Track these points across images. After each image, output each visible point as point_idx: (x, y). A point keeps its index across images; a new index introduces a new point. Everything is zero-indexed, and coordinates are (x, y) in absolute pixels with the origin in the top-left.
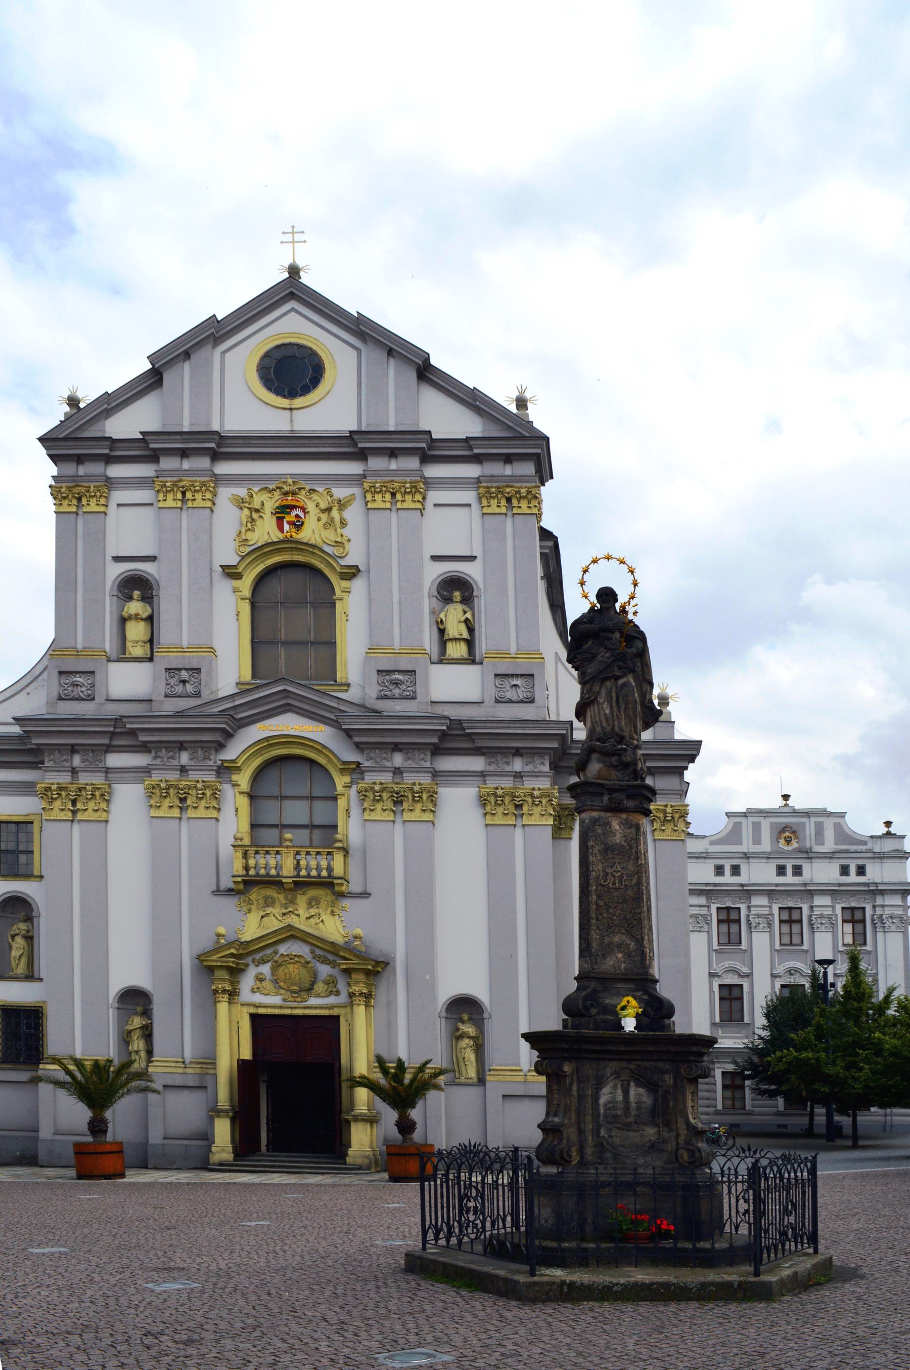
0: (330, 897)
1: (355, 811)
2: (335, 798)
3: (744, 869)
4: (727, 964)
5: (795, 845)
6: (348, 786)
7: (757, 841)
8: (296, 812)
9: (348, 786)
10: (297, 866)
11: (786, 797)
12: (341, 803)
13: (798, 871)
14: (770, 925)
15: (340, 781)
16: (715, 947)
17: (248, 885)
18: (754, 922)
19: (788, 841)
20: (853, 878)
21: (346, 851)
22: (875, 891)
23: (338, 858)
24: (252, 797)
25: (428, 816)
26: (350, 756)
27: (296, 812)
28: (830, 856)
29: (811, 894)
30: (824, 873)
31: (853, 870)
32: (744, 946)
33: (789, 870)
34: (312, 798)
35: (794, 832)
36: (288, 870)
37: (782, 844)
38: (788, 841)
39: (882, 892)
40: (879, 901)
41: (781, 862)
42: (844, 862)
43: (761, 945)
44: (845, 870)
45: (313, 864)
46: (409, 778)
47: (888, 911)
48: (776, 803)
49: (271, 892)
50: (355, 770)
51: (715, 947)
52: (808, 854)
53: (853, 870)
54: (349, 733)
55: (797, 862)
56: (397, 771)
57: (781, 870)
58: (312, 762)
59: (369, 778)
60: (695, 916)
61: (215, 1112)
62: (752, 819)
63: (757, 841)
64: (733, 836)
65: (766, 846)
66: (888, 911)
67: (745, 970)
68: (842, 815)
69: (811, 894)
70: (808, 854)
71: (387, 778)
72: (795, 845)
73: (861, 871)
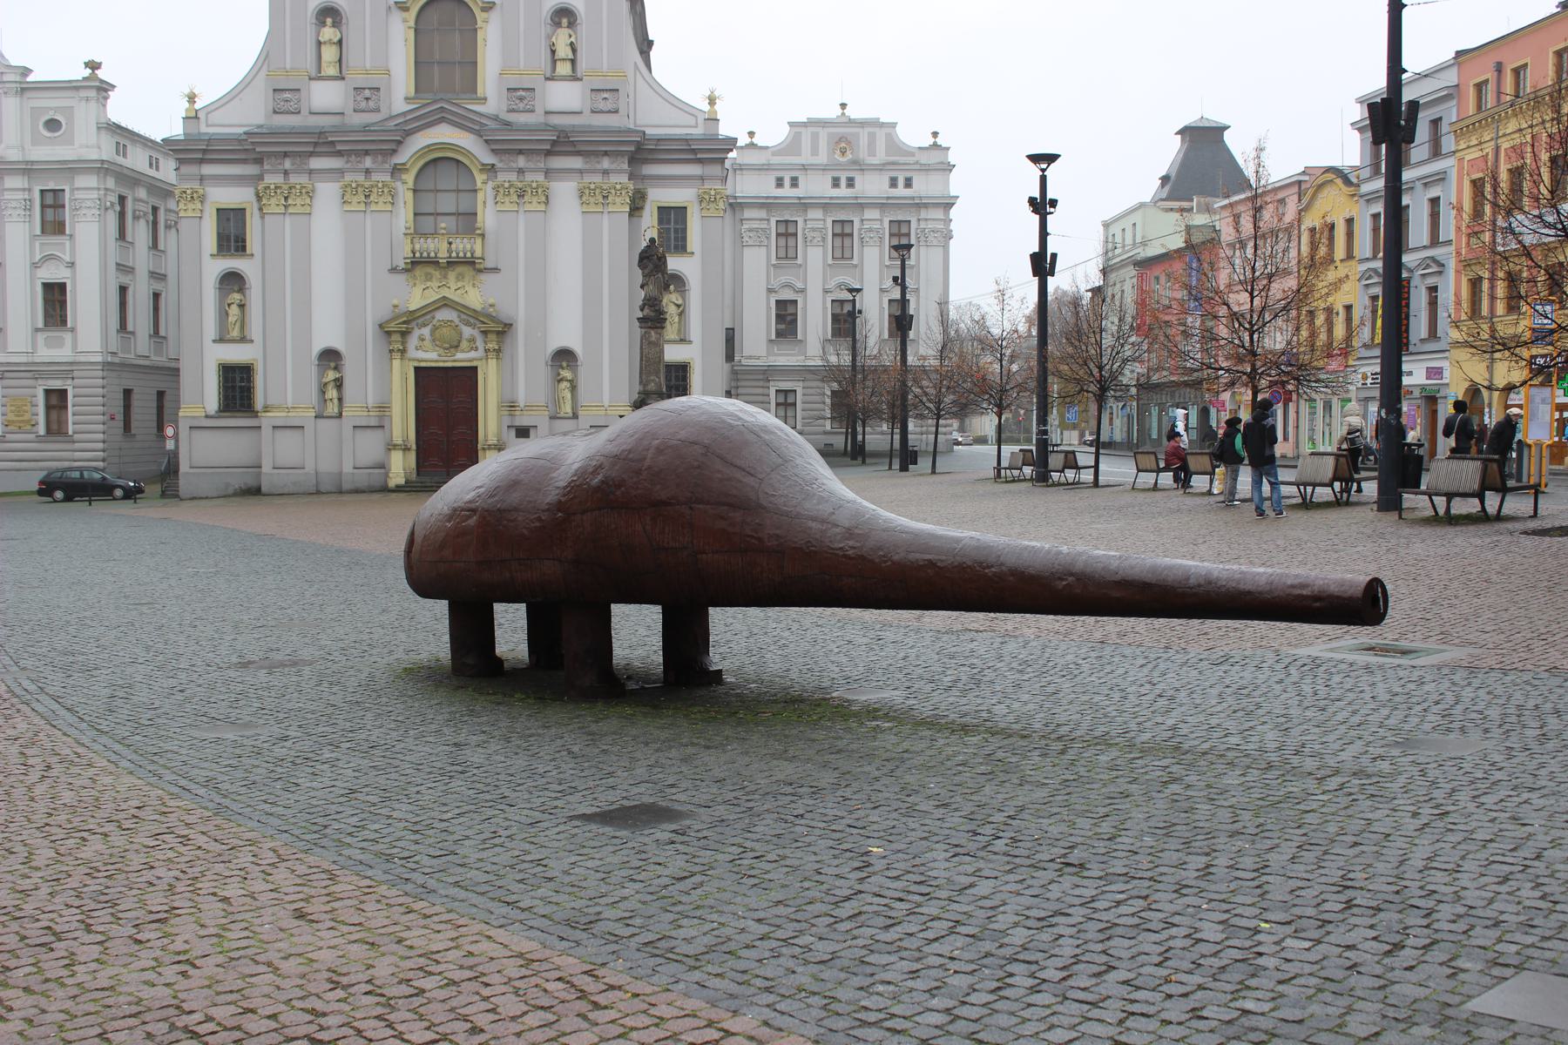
0: (472, 273)
1: (490, 202)
2: (475, 191)
3: (801, 182)
4: (784, 279)
5: (849, 156)
6: (485, 183)
7: (815, 152)
8: (447, 203)
9: (485, 183)
10: (450, 251)
11: (843, 106)
12: (480, 196)
13: (851, 183)
14: (824, 239)
15: (480, 178)
16: (774, 262)
17: (416, 263)
18: (810, 235)
19: (843, 153)
20: (901, 191)
21: (483, 236)
22: (919, 205)
23: (479, 241)
24: (415, 191)
25: (542, 207)
26: (488, 159)
27: (447, 203)
28: (880, 168)
29: (862, 206)
30: (872, 186)
31: (901, 182)
32: (799, 261)
33: (843, 183)
34: (458, 191)
35: (849, 143)
36: (443, 254)
37: (838, 156)
38: (843, 153)
39: (926, 206)
40: (923, 214)
41: (836, 174)
42: (893, 174)
43: (815, 258)
44: (893, 183)
45: (462, 246)
46: (529, 177)
47: (931, 225)
48: (833, 113)
49: (430, 269)
50: (490, 169)
51: (774, 262)
52: (862, 167)
53: (901, 182)
54: (486, 141)
55: (851, 174)
56: (521, 171)
57: (836, 183)
58: (458, 161)
59: (501, 177)
60: (756, 230)
61: (391, 447)
62: (810, 129)
63: (815, 152)
64: (792, 145)
65: (822, 158)
66: (931, 225)
67: (799, 285)
68: (894, 125)
69: (862, 206)
70: (862, 167)
71: (513, 177)
72: (849, 156)
73: (908, 183)
